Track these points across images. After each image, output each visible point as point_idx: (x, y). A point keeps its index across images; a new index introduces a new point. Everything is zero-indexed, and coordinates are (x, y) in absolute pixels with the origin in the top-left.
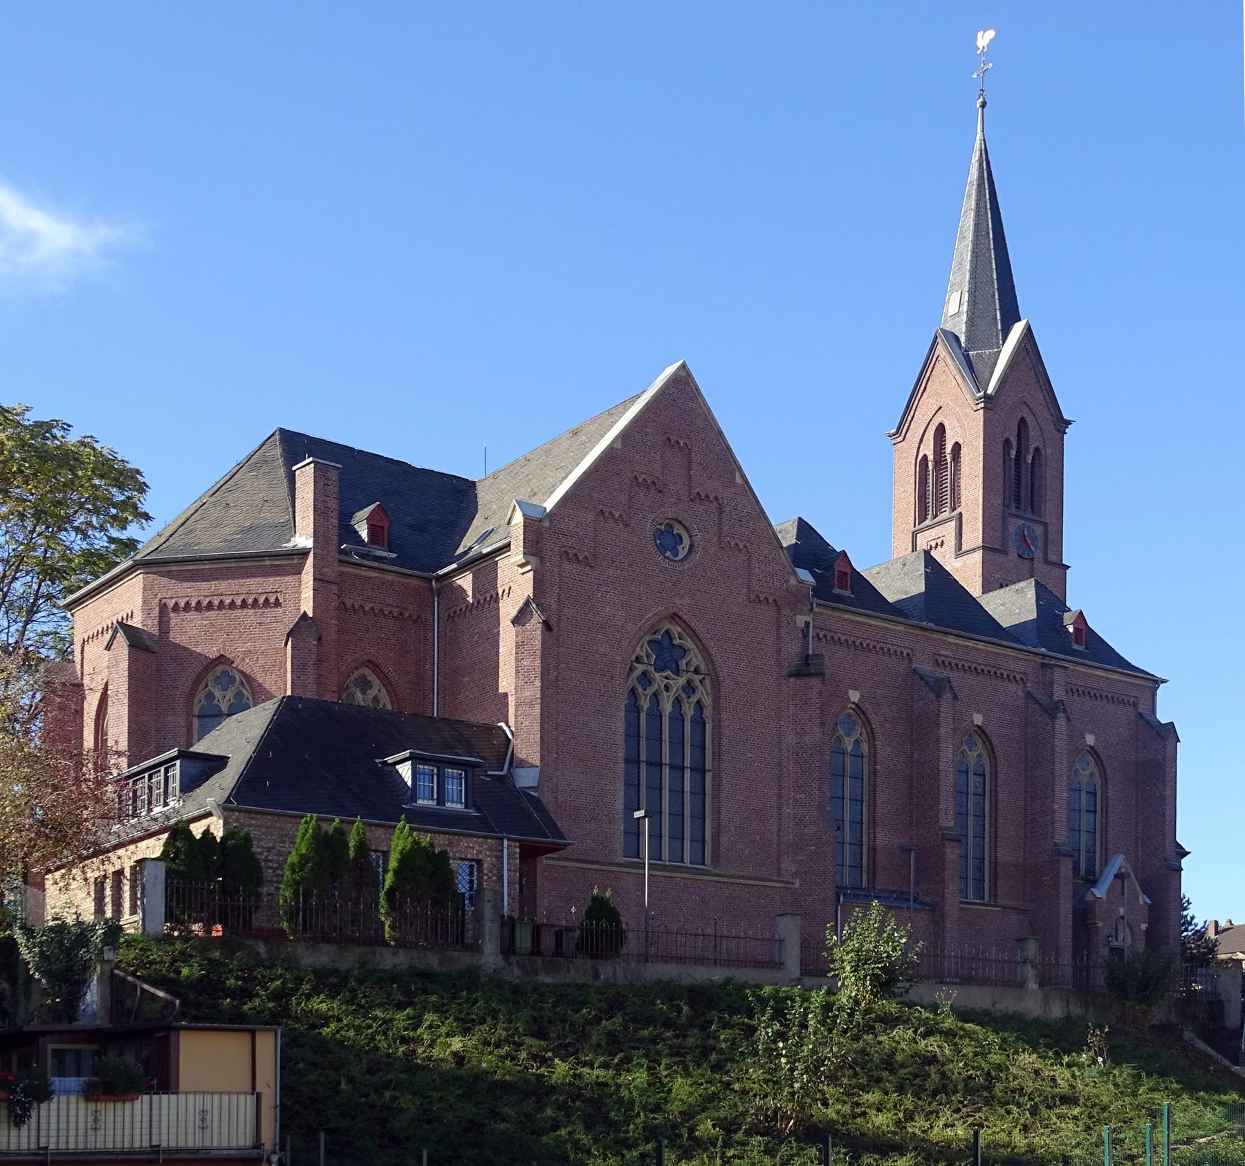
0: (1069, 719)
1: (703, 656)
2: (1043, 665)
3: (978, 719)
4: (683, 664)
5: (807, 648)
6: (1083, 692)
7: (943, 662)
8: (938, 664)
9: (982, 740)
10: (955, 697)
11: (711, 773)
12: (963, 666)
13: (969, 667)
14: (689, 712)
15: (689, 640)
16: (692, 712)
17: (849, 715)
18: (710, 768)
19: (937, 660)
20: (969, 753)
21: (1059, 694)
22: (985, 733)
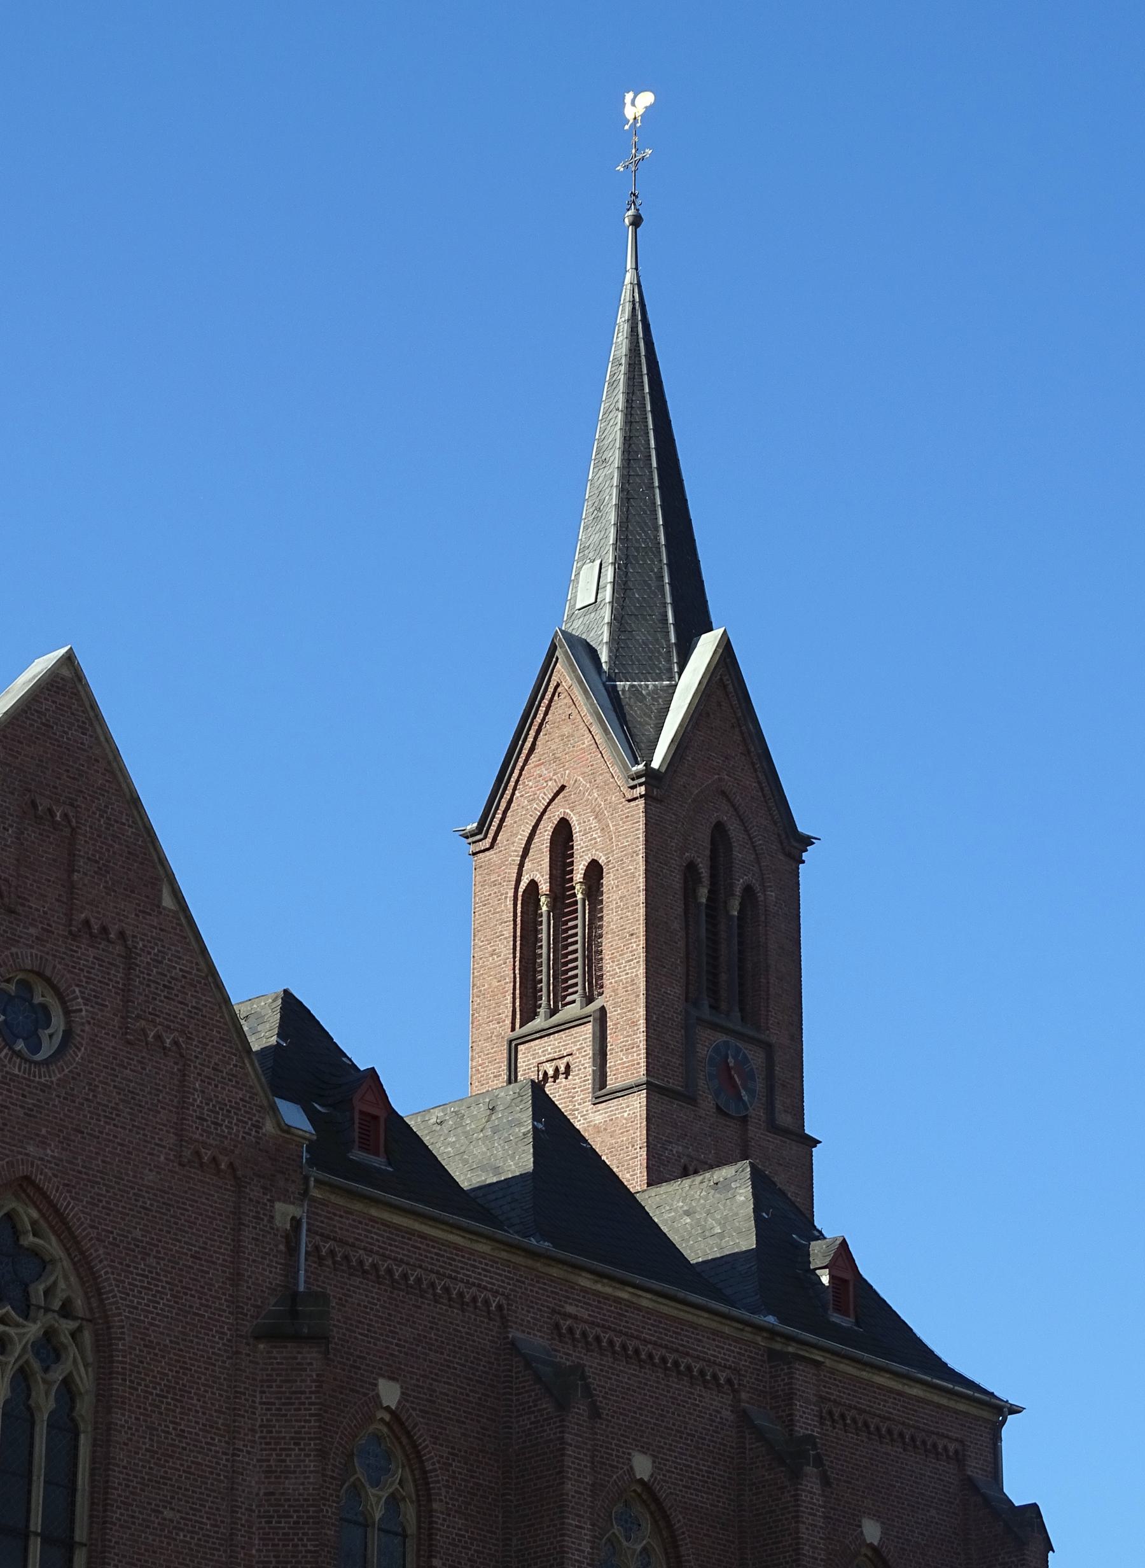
0: (826, 1481)
1: (81, 1278)
2: (772, 1355)
3: (643, 1466)
4: (38, 1289)
5: (296, 1278)
6: (854, 1420)
7: (571, 1330)
8: (560, 1335)
9: (652, 1513)
10: (595, 1413)
11: (84, 1549)
12: (611, 1343)
13: (624, 1347)
14: (45, 1403)
15: (53, 1239)
16: (51, 1404)
17: (377, 1438)
18: (84, 1541)
19: (557, 1326)
20: (625, 1543)
21: (806, 1423)
22: (656, 1500)
